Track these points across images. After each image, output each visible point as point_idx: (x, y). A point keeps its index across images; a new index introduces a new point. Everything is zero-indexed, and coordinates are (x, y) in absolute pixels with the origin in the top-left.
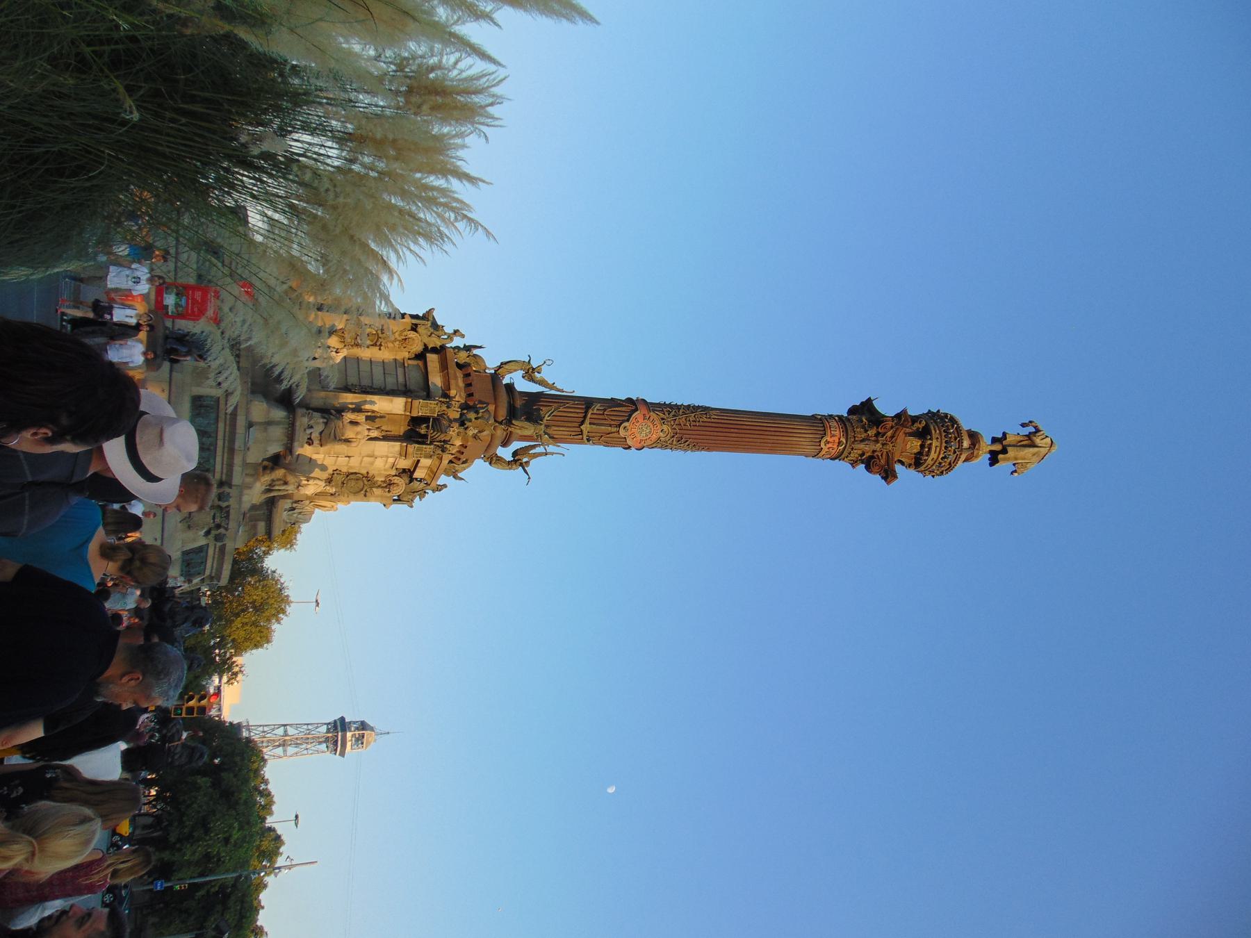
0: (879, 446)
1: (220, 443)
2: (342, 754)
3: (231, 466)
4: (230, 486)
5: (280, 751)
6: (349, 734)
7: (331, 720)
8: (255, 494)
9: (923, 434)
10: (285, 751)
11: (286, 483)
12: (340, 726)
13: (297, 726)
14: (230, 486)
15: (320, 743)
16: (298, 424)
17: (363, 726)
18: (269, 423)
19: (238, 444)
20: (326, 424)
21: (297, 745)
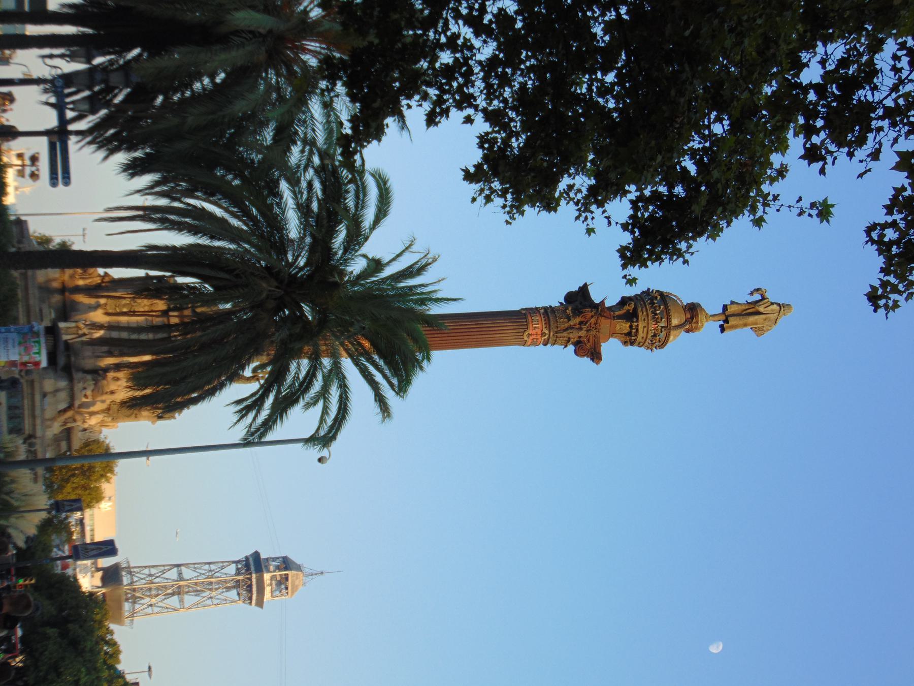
0: (582, 333)
1: (26, 412)
2: (260, 603)
3: (34, 425)
4: (35, 438)
5: (174, 601)
6: (267, 577)
7: (241, 556)
8: (56, 428)
9: (631, 316)
10: (181, 601)
11: (75, 421)
12: (254, 564)
13: (194, 566)
14: (35, 438)
15: (229, 589)
16: (75, 389)
17: (286, 564)
18: (57, 391)
19: (38, 412)
20: (95, 384)
21: (197, 592)
